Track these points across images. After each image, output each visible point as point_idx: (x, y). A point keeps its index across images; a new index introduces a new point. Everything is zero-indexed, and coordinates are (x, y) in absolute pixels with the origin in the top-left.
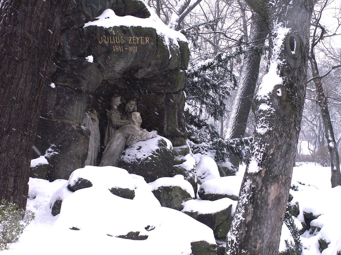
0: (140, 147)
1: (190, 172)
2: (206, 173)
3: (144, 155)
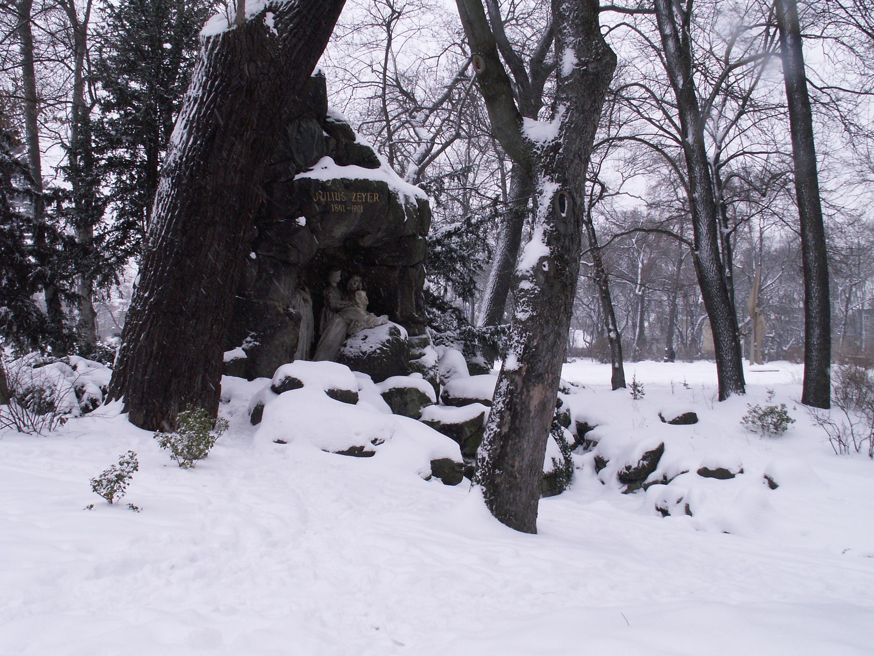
0: (366, 337)
1: (431, 369)
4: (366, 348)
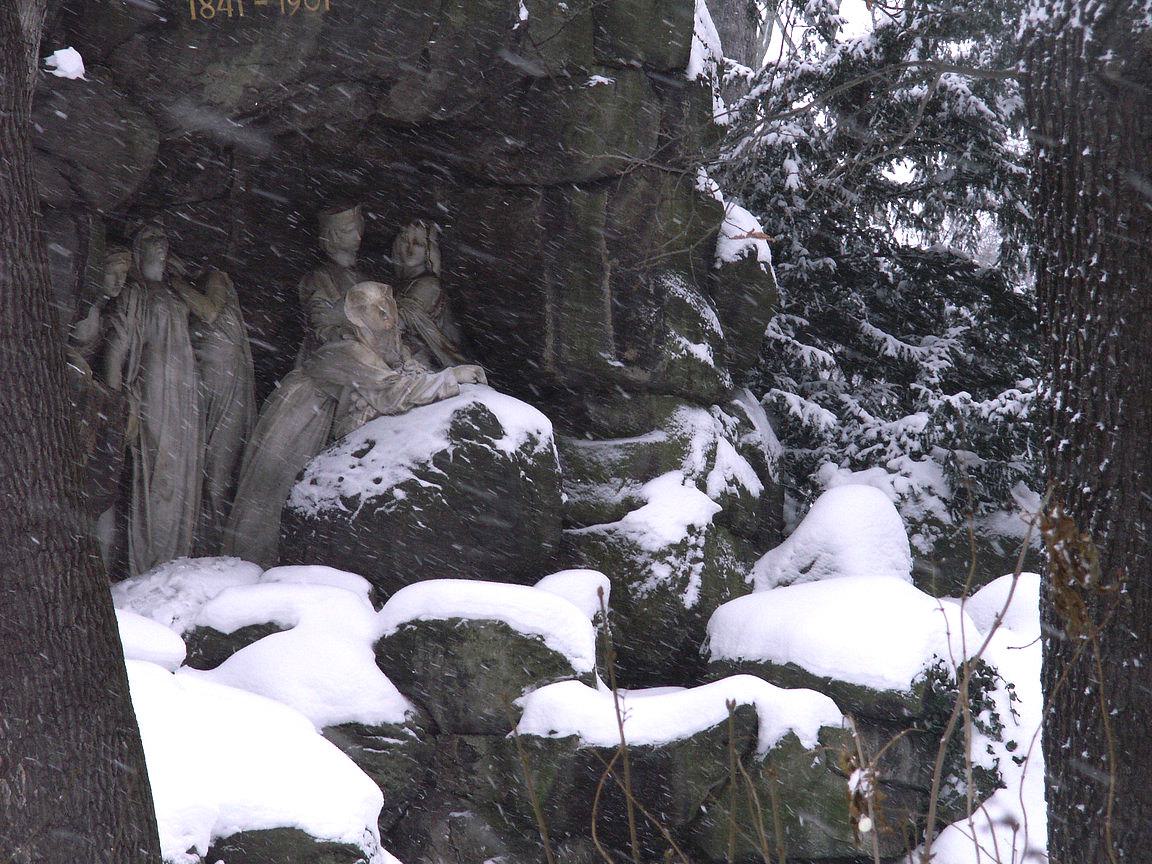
0: (372, 444)
1: (660, 556)
2: (819, 563)
3: (378, 481)
4: (360, 483)
